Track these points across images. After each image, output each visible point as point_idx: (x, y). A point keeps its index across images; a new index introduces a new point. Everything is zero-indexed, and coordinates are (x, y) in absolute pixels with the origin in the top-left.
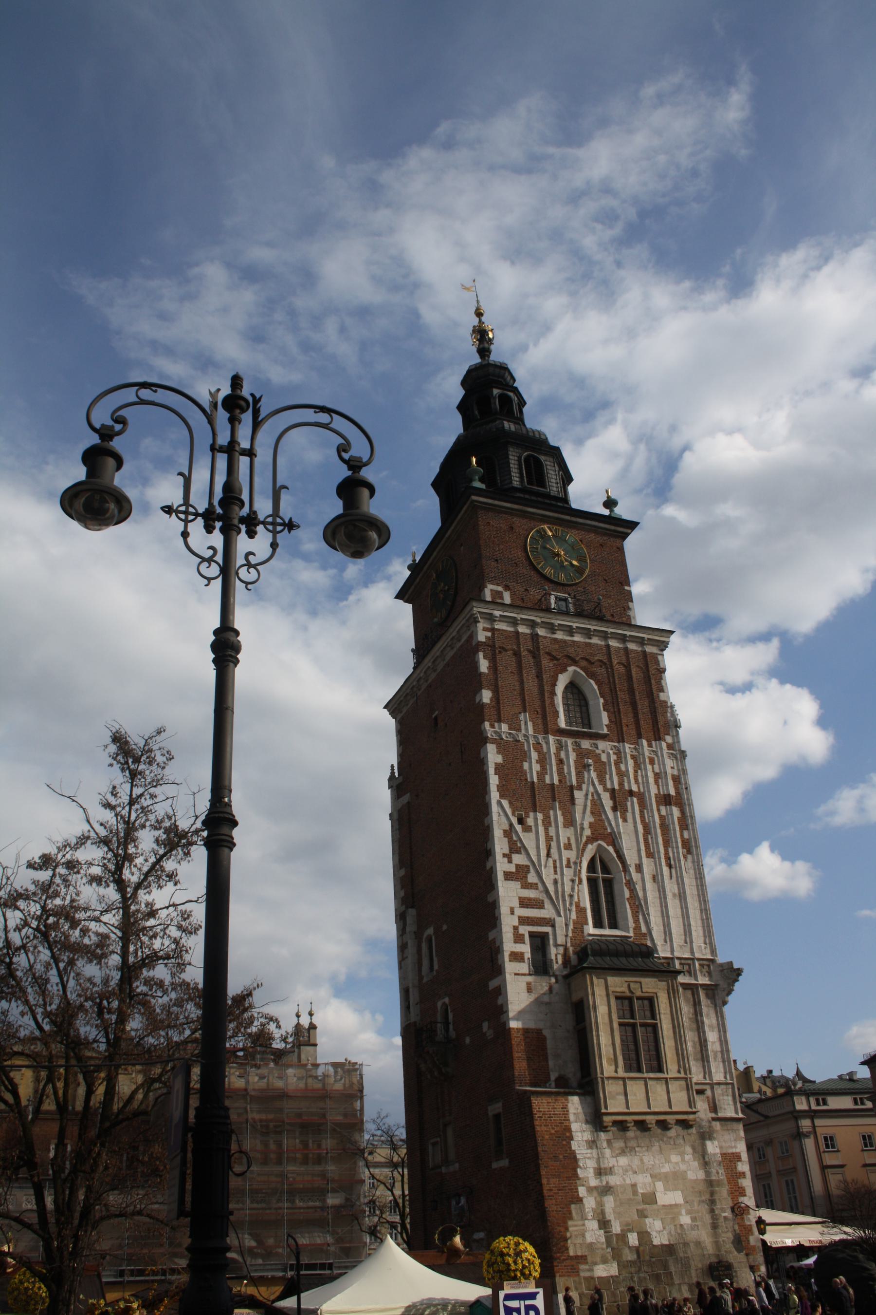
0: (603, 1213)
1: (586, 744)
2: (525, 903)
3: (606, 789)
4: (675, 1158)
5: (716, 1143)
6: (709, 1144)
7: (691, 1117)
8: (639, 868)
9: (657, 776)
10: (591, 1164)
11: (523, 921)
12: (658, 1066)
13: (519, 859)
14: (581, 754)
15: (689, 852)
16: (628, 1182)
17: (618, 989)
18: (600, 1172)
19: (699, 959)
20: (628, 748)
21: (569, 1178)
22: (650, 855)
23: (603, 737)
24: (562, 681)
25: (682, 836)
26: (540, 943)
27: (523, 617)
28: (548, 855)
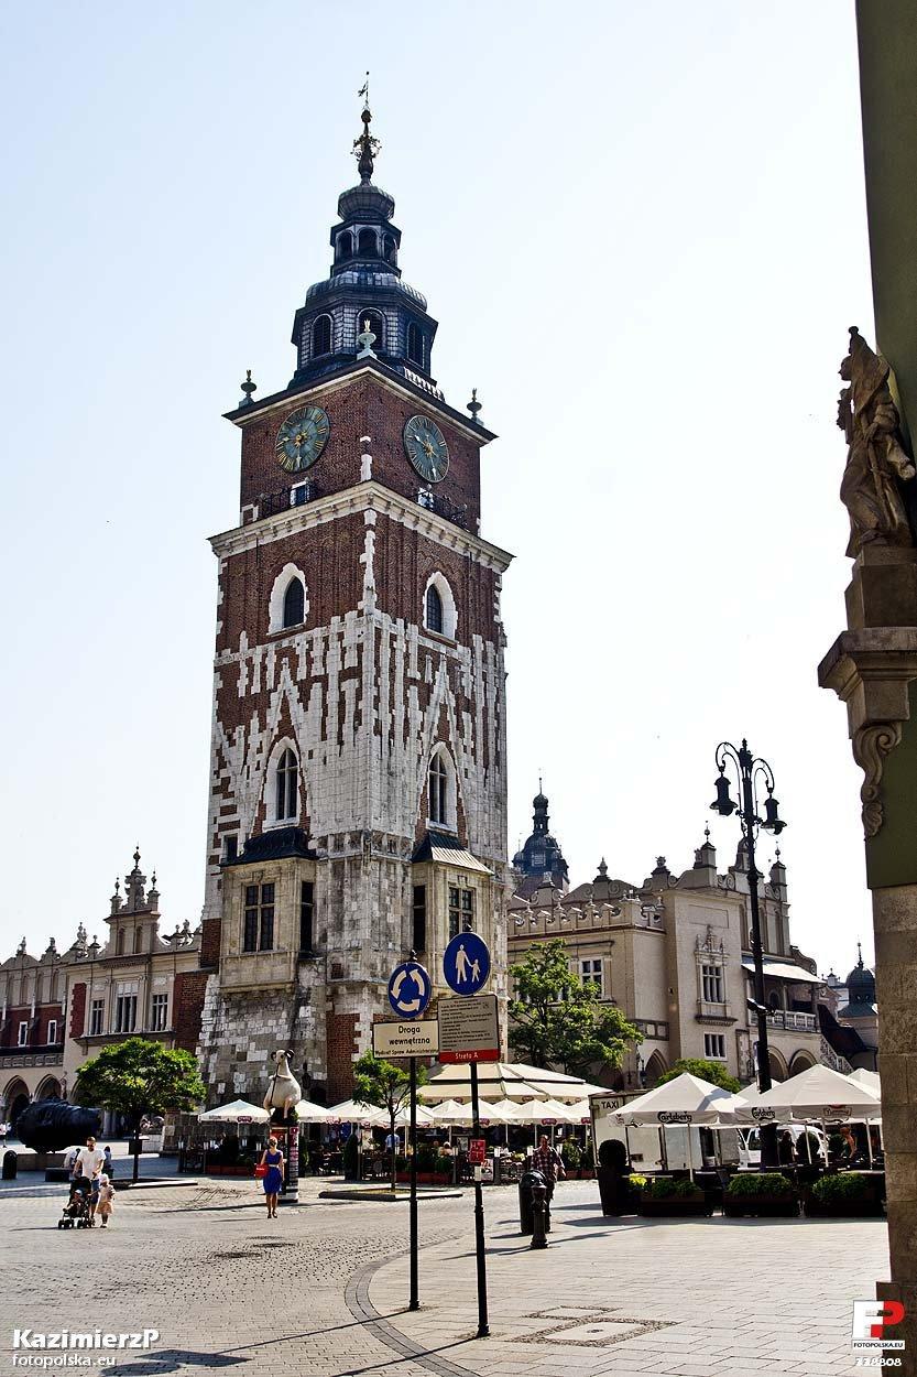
0: (207, 1067)
1: (285, 643)
2: (226, 811)
3: (295, 683)
4: (271, 1023)
5: (309, 1008)
6: (302, 1008)
7: (289, 986)
8: (311, 753)
9: (344, 650)
10: (210, 1029)
11: (223, 827)
12: (267, 943)
13: (223, 773)
14: (280, 654)
15: (360, 724)
16: (231, 1043)
17: (247, 880)
18: (214, 1035)
19: (351, 833)
20: (317, 632)
21: (193, 1041)
22: (324, 738)
23: (306, 629)
24: (280, 585)
25: (357, 707)
26: (231, 843)
27: (246, 534)
28: (245, 763)
